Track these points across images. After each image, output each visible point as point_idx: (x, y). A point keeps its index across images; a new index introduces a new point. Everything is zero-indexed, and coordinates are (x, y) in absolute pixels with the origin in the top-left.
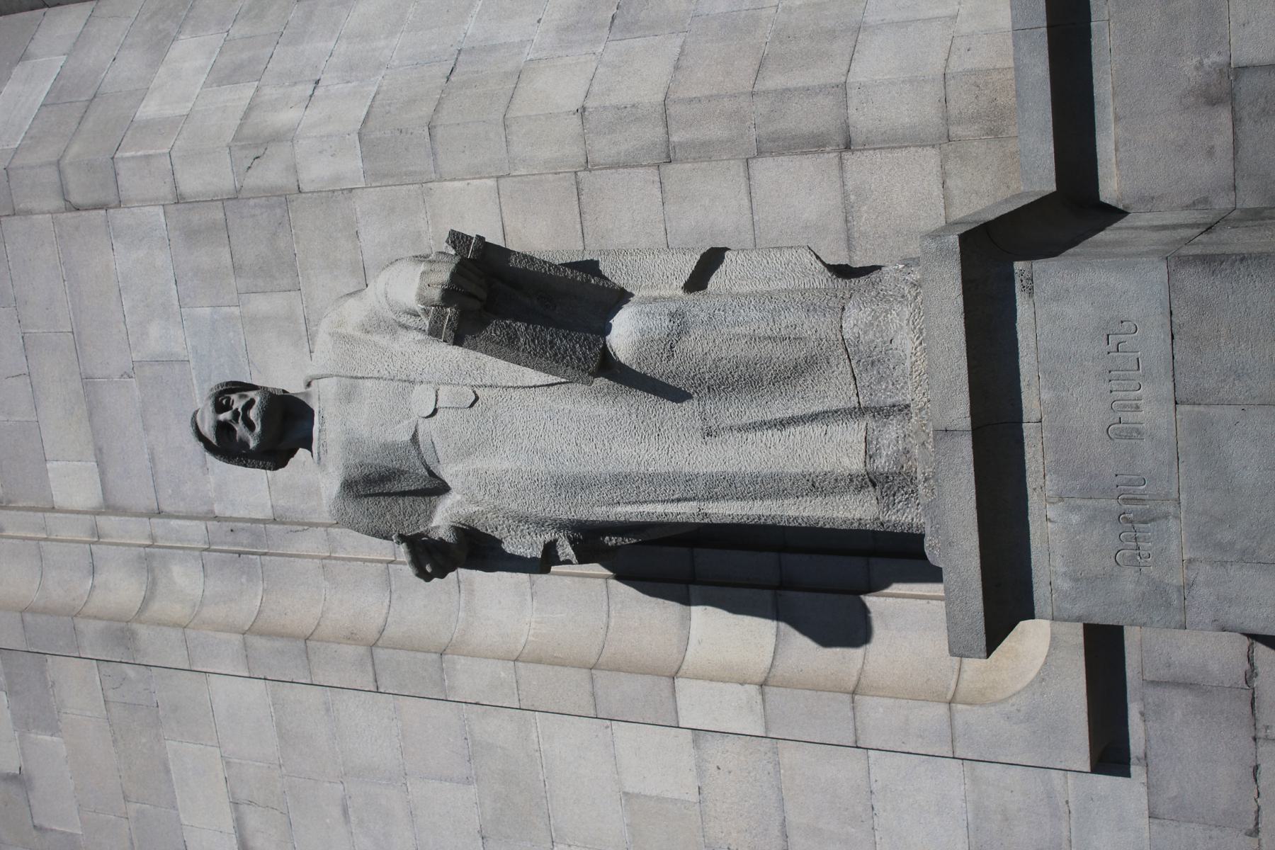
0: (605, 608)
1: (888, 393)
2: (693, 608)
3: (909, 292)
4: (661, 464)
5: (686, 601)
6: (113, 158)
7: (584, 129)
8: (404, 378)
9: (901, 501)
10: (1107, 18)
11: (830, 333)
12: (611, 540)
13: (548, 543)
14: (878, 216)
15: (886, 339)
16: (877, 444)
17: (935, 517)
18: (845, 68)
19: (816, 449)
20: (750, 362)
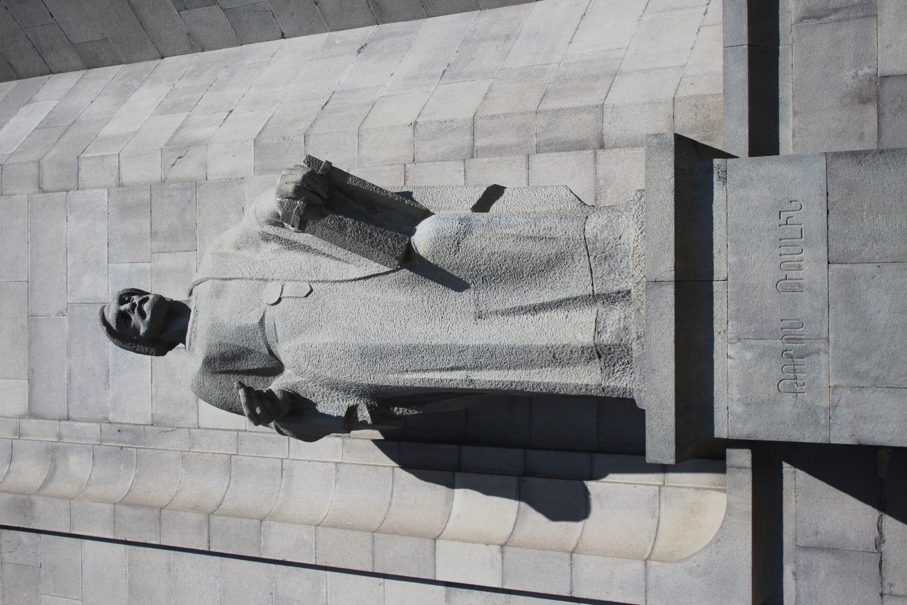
0: (390, 490)
1: (615, 282)
2: (457, 491)
3: (636, 195)
4: (442, 339)
5: (452, 485)
6: (78, 158)
8: (260, 277)
9: (619, 371)
10: (791, 43)
11: (576, 234)
12: (399, 410)
13: (351, 407)
14: (619, 196)
15: (616, 236)
16: (604, 323)
17: (643, 367)
18: (604, 96)
20: (515, 257)
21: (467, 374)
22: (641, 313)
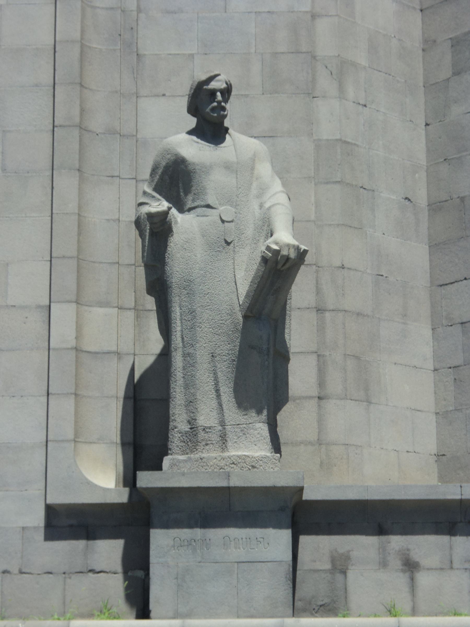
7: (334, 267)
9: (184, 439)
18: (352, 398)
19: (207, 404)
21: (180, 347)
22: (214, 460)
